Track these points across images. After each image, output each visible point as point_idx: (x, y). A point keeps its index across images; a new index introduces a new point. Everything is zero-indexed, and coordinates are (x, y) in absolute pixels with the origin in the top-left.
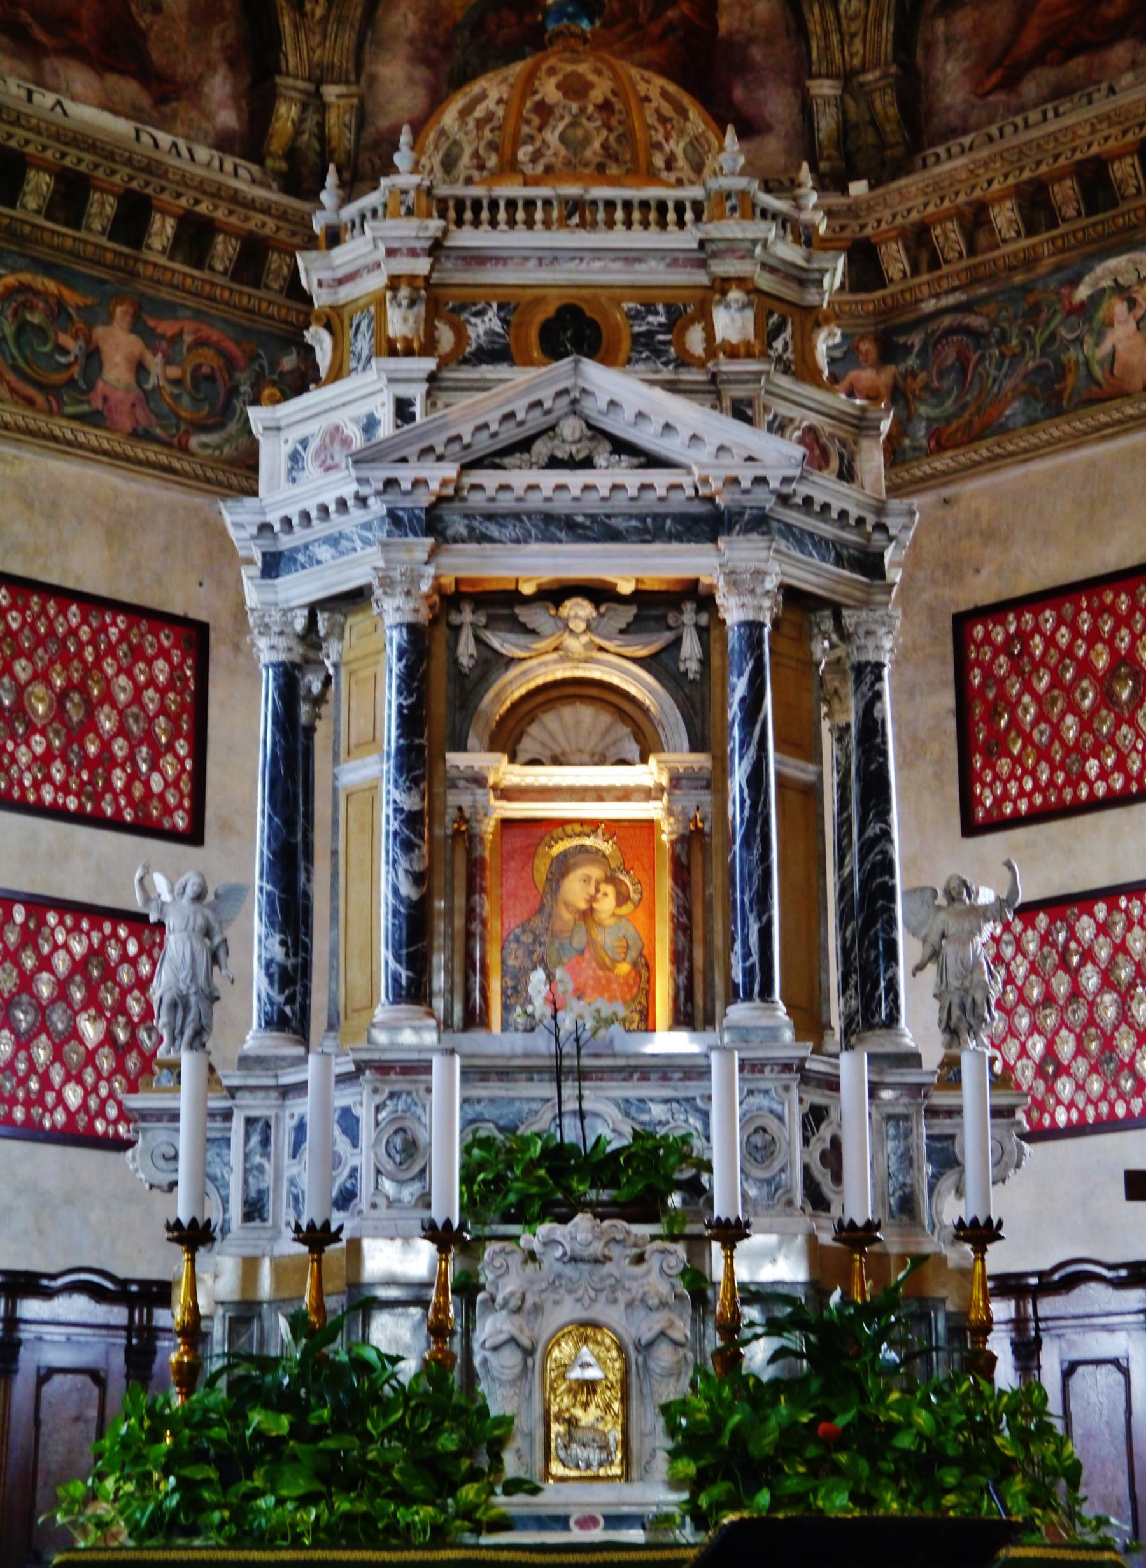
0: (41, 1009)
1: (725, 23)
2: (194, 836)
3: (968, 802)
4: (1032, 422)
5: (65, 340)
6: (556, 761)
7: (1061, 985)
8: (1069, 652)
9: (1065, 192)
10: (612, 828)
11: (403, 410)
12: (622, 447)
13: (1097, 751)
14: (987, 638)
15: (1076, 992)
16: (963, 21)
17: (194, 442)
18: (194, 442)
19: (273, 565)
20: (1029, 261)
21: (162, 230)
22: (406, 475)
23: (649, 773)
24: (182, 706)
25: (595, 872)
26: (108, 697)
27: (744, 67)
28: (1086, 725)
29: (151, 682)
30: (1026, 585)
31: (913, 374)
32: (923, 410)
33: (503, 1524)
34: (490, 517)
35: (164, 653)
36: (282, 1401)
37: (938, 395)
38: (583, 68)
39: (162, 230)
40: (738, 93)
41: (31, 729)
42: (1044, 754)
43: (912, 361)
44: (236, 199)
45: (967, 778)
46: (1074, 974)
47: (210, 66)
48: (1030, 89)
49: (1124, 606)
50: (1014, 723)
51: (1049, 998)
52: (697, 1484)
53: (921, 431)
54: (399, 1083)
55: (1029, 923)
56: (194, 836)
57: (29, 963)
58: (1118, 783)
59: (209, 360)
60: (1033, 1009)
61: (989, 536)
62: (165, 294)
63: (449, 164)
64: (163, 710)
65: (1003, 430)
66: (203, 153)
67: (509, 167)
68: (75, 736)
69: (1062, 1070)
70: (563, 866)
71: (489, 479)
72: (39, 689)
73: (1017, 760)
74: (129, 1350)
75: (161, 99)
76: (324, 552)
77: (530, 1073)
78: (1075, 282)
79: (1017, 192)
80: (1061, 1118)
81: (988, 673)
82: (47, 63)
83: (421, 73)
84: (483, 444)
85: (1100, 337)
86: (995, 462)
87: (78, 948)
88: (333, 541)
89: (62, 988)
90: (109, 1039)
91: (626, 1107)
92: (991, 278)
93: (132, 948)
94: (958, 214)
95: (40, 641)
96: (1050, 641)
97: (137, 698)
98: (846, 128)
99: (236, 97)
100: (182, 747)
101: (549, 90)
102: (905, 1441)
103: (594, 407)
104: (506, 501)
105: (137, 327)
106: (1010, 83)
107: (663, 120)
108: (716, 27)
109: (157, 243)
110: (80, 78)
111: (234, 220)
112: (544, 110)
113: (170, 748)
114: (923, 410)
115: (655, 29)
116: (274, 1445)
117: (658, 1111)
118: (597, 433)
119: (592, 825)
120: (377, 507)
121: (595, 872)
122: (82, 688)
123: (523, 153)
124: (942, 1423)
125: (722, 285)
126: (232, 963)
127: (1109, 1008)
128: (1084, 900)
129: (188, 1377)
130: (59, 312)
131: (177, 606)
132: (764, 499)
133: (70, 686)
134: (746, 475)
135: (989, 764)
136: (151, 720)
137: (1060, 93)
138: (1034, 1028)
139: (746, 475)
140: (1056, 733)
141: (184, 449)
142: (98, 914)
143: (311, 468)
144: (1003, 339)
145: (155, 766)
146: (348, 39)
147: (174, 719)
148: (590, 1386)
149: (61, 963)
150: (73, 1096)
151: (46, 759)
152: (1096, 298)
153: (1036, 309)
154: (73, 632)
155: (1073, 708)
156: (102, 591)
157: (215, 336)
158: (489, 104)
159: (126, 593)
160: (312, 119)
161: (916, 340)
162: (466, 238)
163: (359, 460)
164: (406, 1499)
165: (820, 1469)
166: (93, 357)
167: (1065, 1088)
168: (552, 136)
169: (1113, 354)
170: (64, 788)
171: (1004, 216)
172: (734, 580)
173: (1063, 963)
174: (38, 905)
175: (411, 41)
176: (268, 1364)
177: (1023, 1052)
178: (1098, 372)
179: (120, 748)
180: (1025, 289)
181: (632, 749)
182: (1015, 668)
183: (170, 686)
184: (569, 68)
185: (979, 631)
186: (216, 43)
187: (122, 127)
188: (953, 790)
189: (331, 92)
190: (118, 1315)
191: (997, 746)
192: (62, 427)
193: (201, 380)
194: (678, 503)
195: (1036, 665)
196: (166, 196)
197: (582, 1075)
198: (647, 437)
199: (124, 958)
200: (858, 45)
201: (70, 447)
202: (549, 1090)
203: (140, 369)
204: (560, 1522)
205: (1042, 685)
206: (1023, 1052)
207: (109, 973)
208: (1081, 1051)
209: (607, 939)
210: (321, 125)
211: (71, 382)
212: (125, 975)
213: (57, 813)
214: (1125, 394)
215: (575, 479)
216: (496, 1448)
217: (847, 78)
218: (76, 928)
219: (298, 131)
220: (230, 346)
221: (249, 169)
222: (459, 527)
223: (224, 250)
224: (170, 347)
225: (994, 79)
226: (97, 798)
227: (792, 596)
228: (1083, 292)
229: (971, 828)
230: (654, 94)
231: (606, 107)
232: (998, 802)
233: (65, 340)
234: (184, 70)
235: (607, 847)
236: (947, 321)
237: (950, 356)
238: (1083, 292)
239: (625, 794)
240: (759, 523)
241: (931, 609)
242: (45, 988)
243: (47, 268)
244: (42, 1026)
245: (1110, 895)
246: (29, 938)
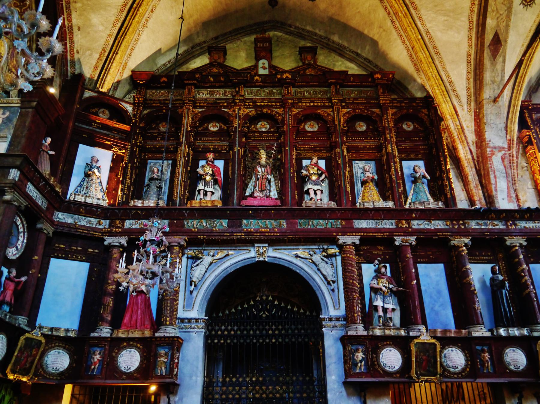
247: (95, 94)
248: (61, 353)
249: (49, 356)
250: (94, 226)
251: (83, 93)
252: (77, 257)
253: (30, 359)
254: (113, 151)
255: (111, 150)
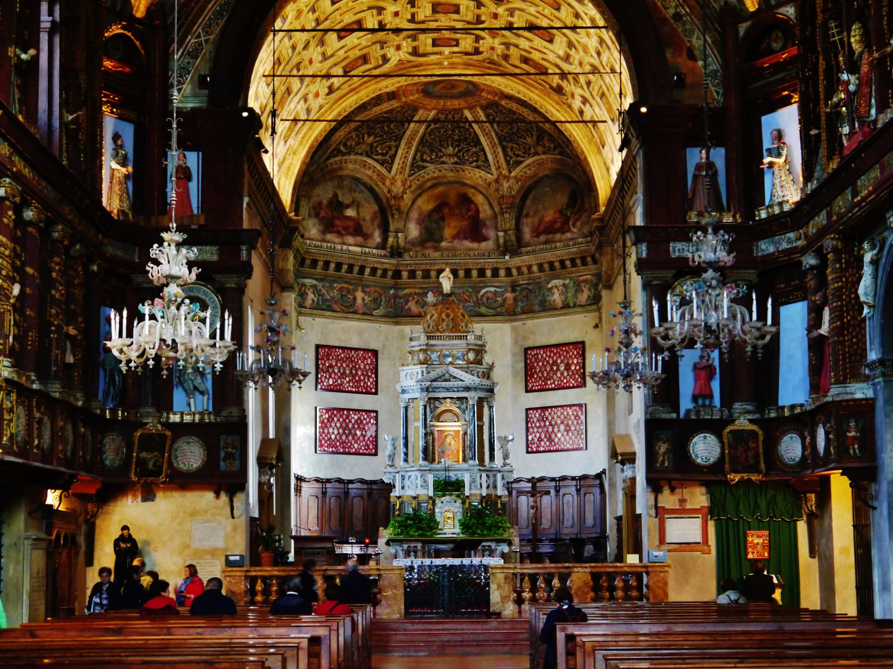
0: (350, 430)
1: (481, 215)
2: (376, 393)
3: (527, 386)
4: (540, 311)
5: (350, 296)
6: (445, 422)
7: (542, 424)
8: (545, 359)
9: (546, 266)
10: (453, 431)
11: (423, 372)
12: (455, 378)
13: (550, 380)
14: (531, 354)
15: (545, 426)
16: (529, 220)
17: (374, 313)
18: (374, 313)
19: (403, 392)
20: (540, 278)
21: (368, 271)
22: (423, 383)
23: (458, 424)
24: (373, 368)
25: (451, 437)
26: (360, 368)
27: (485, 225)
28: (548, 374)
29: (367, 364)
30: (538, 344)
31: (518, 296)
32: (520, 304)
33: (439, 534)
34: (436, 388)
35: (369, 357)
36: (411, 519)
37: (523, 301)
38: (449, 311)
39: (368, 271)
40: (484, 231)
41: (346, 376)
42: (540, 378)
43: (517, 293)
44: (382, 263)
45: (526, 381)
46: (545, 422)
47: (375, 229)
48: (542, 238)
49: (555, 351)
50: (535, 371)
51: (540, 426)
52: (462, 529)
53: (519, 309)
54: (423, 472)
55: (537, 411)
56: (376, 393)
57: (347, 421)
58: (553, 386)
59: (376, 295)
60: (537, 428)
61: (532, 332)
62: (368, 283)
63: (429, 326)
64: (370, 369)
65: (534, 312)
66: (374, 251)
67: (438, 330)
68: (354, 376)
69: (542, 440)
70: (446, 436)
71: (435, 384)
72: (347, 368)
73: (536, 379)
74: (368, 493)
75: (366, 240)
76: (411, 391)
77: (442, 470)
78: (548, 283)
79: (538, 264)
80: (542, 449)
81: (531, 360)
82: (345, 237)
83: (418, 226)
84: (434, 378)
85: (552, 296)
86: (532, 318)
87: (356, 417)
88: (412, 390)
89: (353, 425)
90: (362, 435)
91: (455, 475)
92: (532, 279)
93: (366, 417)
94: (527, 266)
95: (347, 359)
96: (542, 356)
97: (365, 367)
98: (505, 241)
99: (380, 235)
100: (373, 376)
101: (444, 316)
102: (488, 524)
103: (451, 372)
104: (438, 386)
105: (363, 291)
106: (538, 236)
107: (461, 320)
108: (479, 216)
109: (366, 274)
110: (350, 239)
111: (381, 267)
112: (443, 320)
113: (371, 376)
114: (520, 304)
115: (466, 217)
116: (411, 525)
117: (460, 475)
118: (451, 375)
119: (450, 431)
120: (419, 387)
121: (451, 437)
122: (355, 367)
123: (440, 327)
124: (492, 522)
125: (470, 350)
126: (398, 448)
127: (550, 429)
128: (546, 408)
129: (399, 515)
130: (348, 291)
131: (371, 348)
132: (475, 386)
133: (353, 367)
134: (472, 383)
135: (531, 379)
136: (367, 371)
137: (546, 242)
138: (538, 432)
139: (472, 383)
140: (543, 375)
141: (372, 315)
142: (359, 411)
143: (408, 378)
144: (535, 292)
145: (369, 380)
146: (403, 222)
147: (372, 370)
148: (449, 518)
149: (353, 421)
150: (356, 446)
151: (349, 382)
152: (552, 288)
153: (540, 288)
154: (353, 356)
155: (546, 370)
156: (358, 347)
157: (377, 289)
158: (434, 317)
159: (362, 347)
160: (396, 240)
161: (519, 289)
162: (432, 342)
163: (417, 382)
164: (427, 531)
165: (477, 528)
166: (355, 299)
167: (542, 443)
168: (444, 324)
169: (554, 300)
170: (352, 387)
171: (535, 268)
172: (471, 398)
173: (543, 420)
174: (349, 410)
175: (416, 219)
176: (409, 514)
177: (535, 436)
178: (552, 303)
179: (362, 378)
180: (539, 283)
181: (456, 420)
182: (536, 361)
183: (371, 364)
184: (447, 311)
185: (529, 352)
186: (376, 224)
187: (358, 249)
188: (524, 383)
189: (400, 235)
190: (366, 486)
191: (532, 376)
192: (350, 315)
193: (375, 299)
194: (463, 386)
195: (540, 360)
196: (368, 265)
197: (449, 470)
198: (458, 376)
199: (364, 419)
200: (508, 224)
201: (351, 319)
202: (444, 473)
203: (363, 299)
204: (446, 534)
205: (541, 364)
206: (535, 436)
207: (362, 422)
208: (545, 437)
209: (453, 447)
210: (398, 241)
211: (351, 305)
212: (364, 422)
213: (351, 392)
214: (556, 309)
215: (448, 383)
216: (438, 525)
217: (505, 231)
218: (355, 414)
219: (393, 242)
220: (381, 291)
221: (383, 252)
222: (431, 390)
223: (379, 272)
224: (368, 293)
225: (535, 234)
226: (358, 388)
227: (479, 398)
228: (550, 286)
229: (527, 391)
230: (459, 314)
231: (452, 319)
232: (533, 386)
233: (350, 296)
234: (370, 232)
235: (453, 433)
236: (525, 286)
237: (525, 293)
238: (550, 286)
239: (456, 426)
240: (475, 389)
241: (521, 346)
242: (350, 426)
243: (346, 282)
244: (350, 433)
245: (551, 407)
246: (347, 417)
247: (748, 24)
248: (794, 439)
249: (782, 445)
250: (794, 245)
251: (737, 32)
252: (797, 297)
253: (750, 454)
254: (795, 102)
255: (792, 104)
